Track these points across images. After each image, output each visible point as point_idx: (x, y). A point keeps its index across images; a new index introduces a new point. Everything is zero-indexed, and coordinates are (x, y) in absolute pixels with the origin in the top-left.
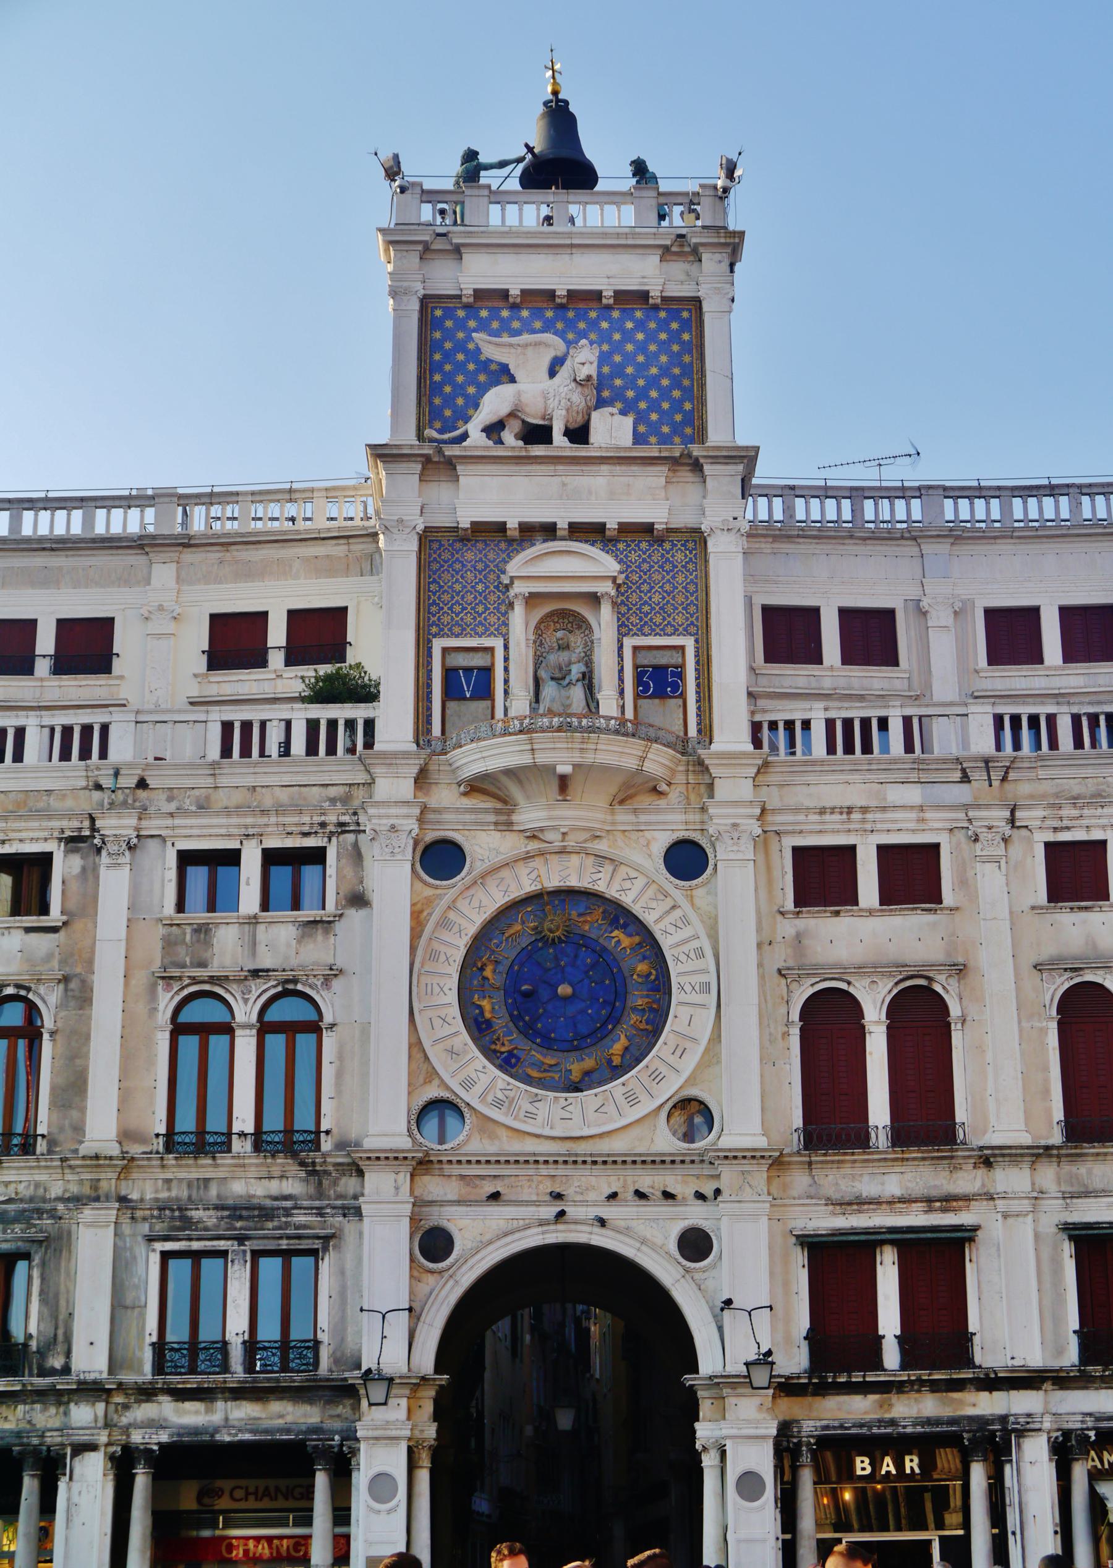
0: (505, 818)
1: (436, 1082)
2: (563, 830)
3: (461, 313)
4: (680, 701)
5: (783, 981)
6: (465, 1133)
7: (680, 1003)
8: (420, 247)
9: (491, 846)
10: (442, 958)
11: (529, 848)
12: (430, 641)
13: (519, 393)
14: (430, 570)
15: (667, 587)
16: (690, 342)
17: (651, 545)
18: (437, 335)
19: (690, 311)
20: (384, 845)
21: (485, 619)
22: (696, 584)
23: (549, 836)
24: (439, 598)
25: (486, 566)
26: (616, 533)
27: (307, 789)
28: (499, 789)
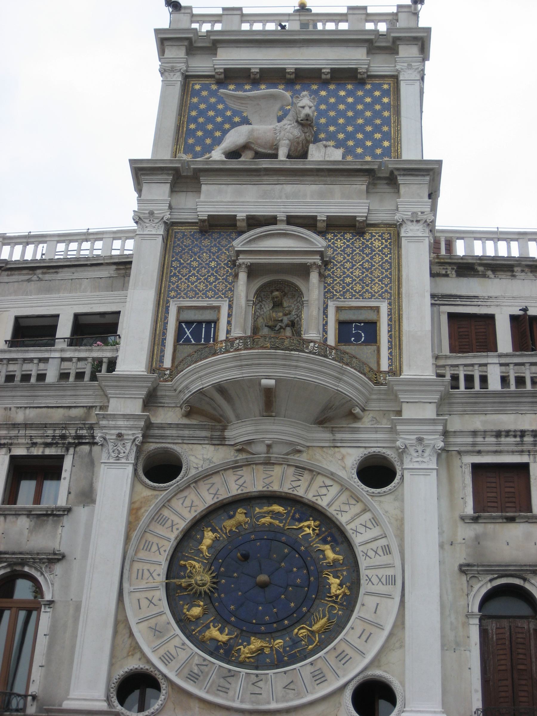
0: (219, 433)
1: (138, 655)
2: (269, 442)
3: (214, 87)
5: (464, 578)
6: (160, 702)
7: (368, 594)
8: (186, 43)
9: (205, 456)
10: (154, 548)
11: (238, 458)
12: (168, 302)
13: (253, 130)
14: (173, 252)
15: (366, 265)
16: (389, 104)
18: (195, 100)
19: (389, 84)
20: (111, 451)
21: (215, 287)
22: (390, 263)
23: (255, 448)
25: (220, 250)
26: (325, 224)
27: (54, 410)
28: (214, 409)
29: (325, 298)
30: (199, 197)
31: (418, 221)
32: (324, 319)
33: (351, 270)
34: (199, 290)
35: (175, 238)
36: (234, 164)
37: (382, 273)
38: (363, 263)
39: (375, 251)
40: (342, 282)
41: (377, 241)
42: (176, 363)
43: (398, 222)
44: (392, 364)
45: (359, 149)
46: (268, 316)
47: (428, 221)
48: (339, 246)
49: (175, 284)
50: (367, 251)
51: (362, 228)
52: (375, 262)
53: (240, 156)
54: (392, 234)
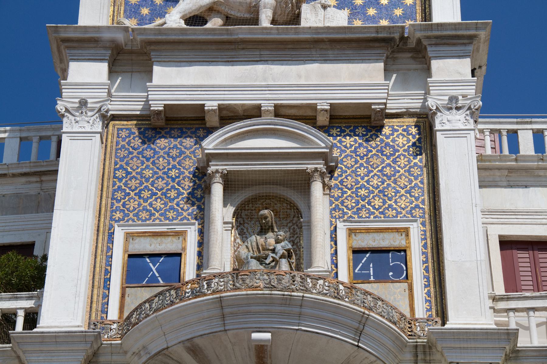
4: (405, 285)
12: (111, 227)
15: (388, 171)
17: (368, 131)
24: (126, 184)
29: (332, 217)
30: (151, 81)
31: (458, 108)
32: (332, 247)
33: (366, 178)
34: (155, 209)
35: (118, 137)
36: (197, 32)
37: (410, 182)
38: (383, 168)
39: (398, 151)
40: (354, 195)
41: (401, 137)
42: (126, 314)
43: (431, 110)
44: (431, 308)
45: (371, 9)
46: (254, 244)
47: (472, 107)
48: (348, 145)
49: (120, 201)
50: (388, 151)
51: (380, 120)
52: (399, 166)
53: (205, 22)
54: (422, 127)
